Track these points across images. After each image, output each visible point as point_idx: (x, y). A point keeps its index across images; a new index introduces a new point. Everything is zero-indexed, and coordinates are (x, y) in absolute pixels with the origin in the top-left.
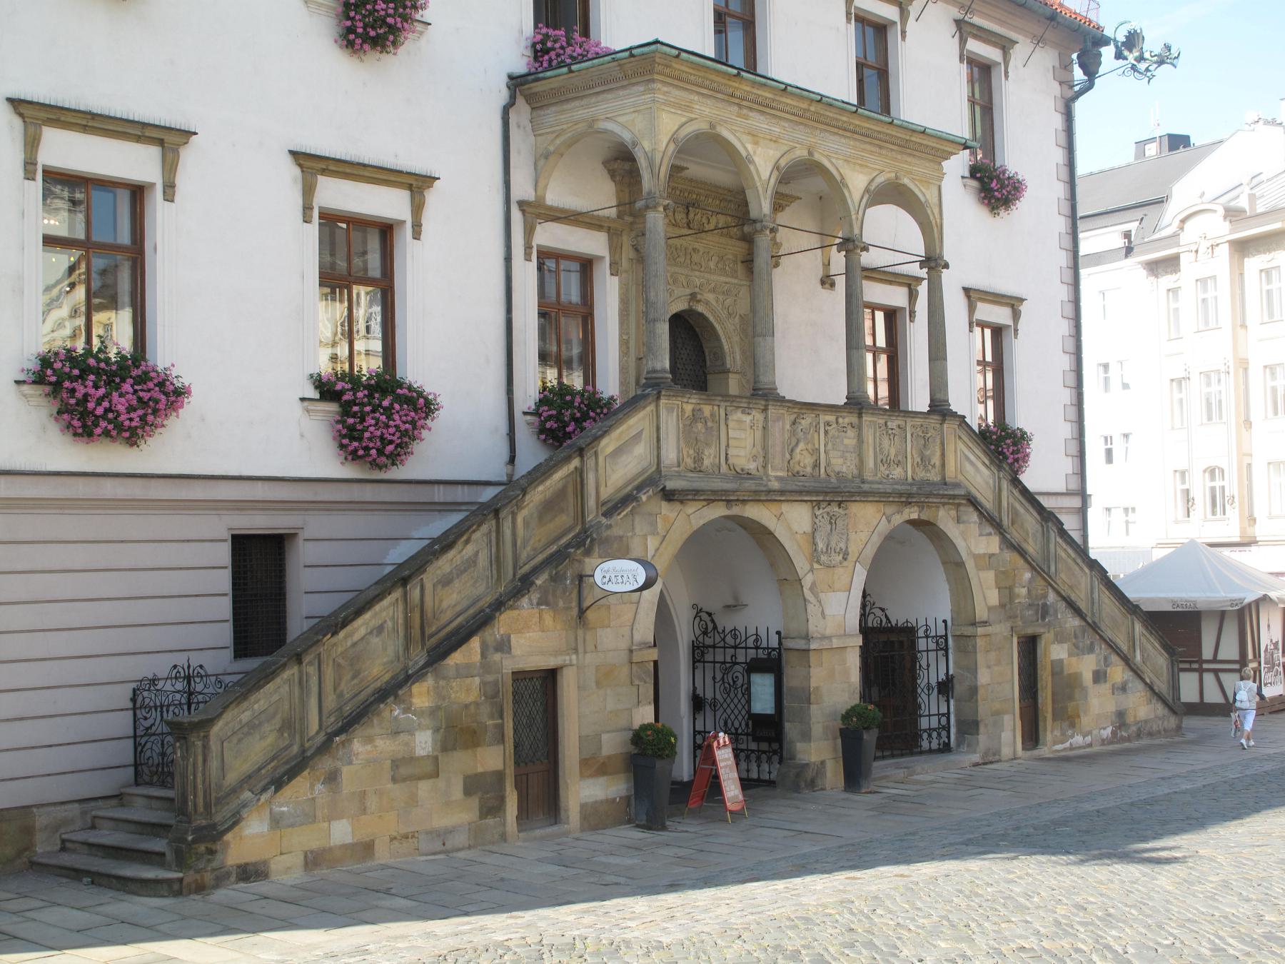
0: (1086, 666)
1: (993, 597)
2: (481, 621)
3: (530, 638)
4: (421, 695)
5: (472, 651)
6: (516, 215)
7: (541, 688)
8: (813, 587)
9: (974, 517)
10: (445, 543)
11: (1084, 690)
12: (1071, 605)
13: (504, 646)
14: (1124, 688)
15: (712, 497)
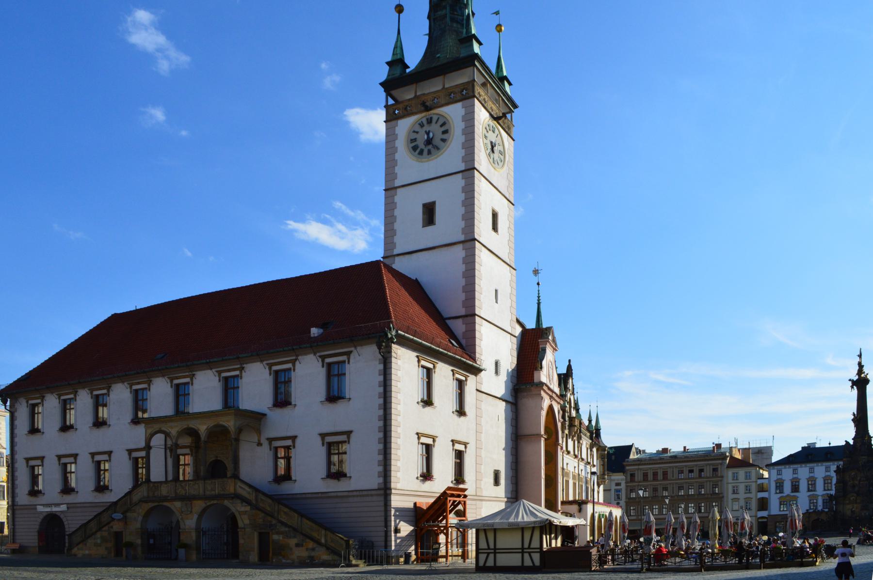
0: (293, 542)
1: (247, 522)
2: (108, 523)
3: (117, 527)
4: (98, 535)
5: (106, 528)
6: (168, 451)
7: (118, 535)
8: (182, 519)
9: (239, 501)
10: (104, 511)
11: (291, 549)
12: (283, 523)
13: (112, 527)
14: (313, 549)
15: (153, 501)
